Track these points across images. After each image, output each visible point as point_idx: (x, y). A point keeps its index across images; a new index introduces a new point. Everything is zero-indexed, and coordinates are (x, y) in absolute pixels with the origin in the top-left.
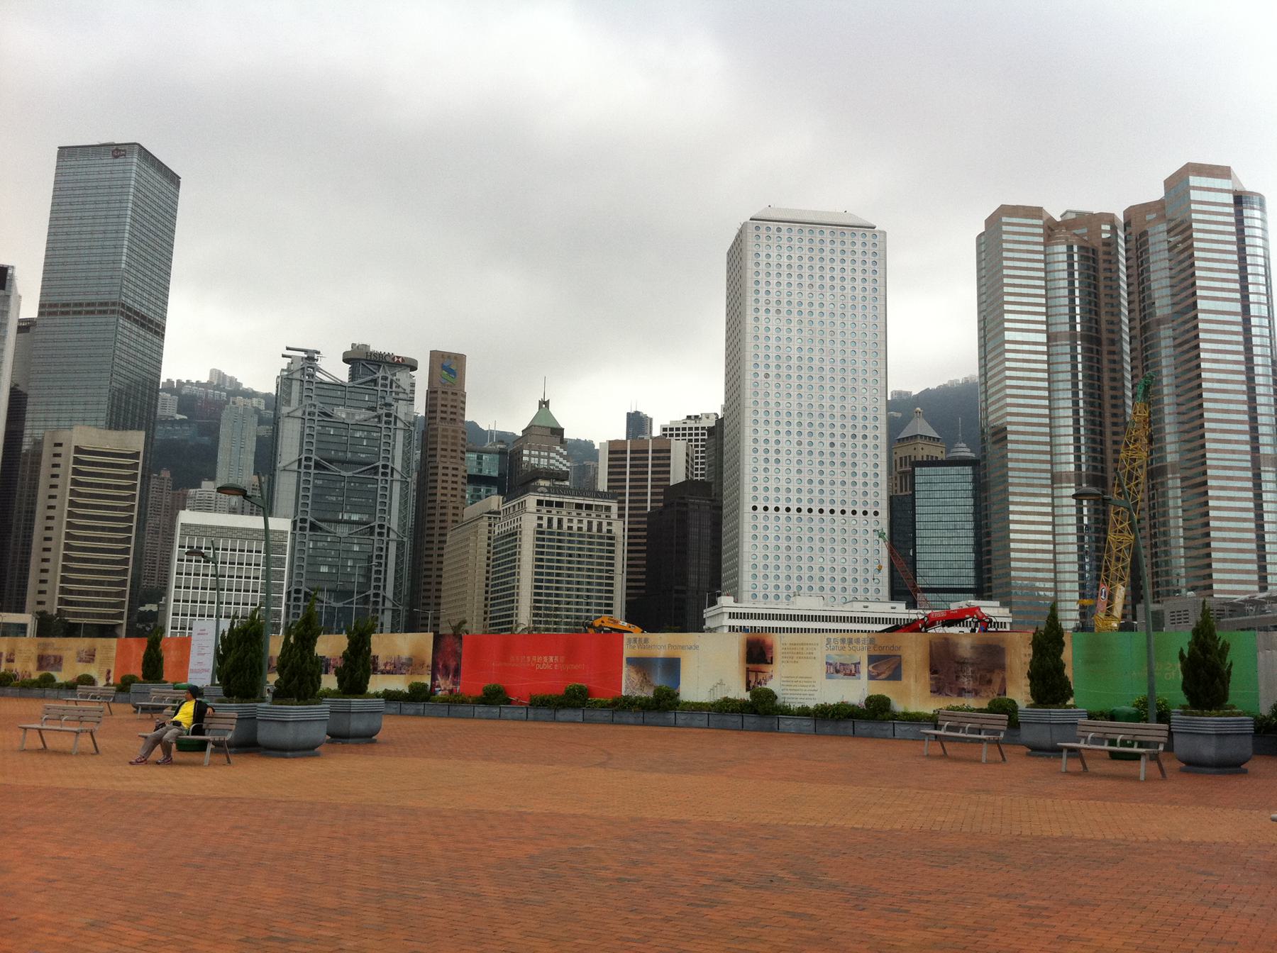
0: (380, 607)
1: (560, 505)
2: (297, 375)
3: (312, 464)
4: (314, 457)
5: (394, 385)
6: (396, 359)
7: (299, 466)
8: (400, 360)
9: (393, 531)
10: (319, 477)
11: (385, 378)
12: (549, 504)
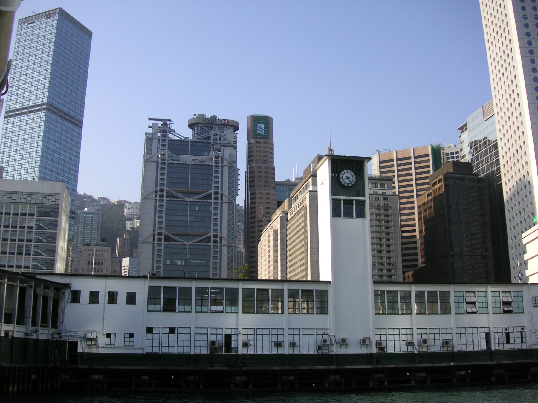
3: (165, 193)
5: (222, 139)
6: (223, 121)
8: (226, 122)
10: (170, 202)
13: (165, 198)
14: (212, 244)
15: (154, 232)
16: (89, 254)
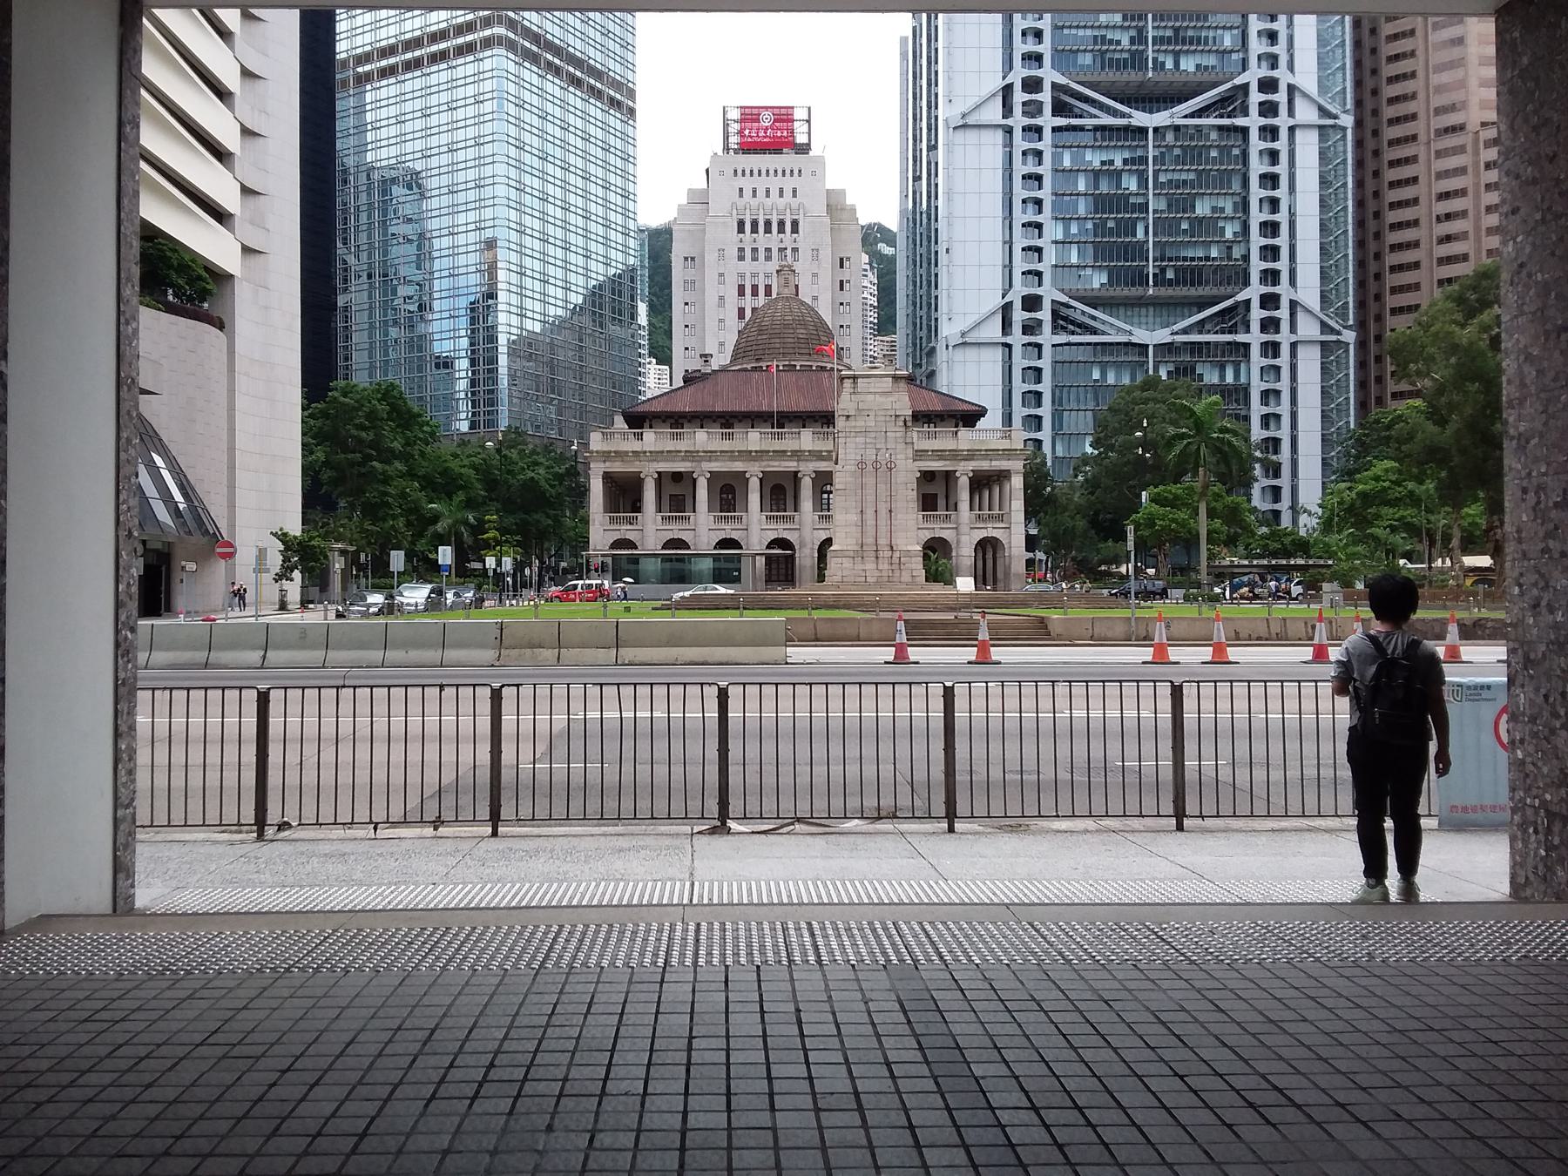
0: (1284, 337)
9: (1305, 95)
14: (1253, 121)
15: (1004, 78)
16: (741, 190)
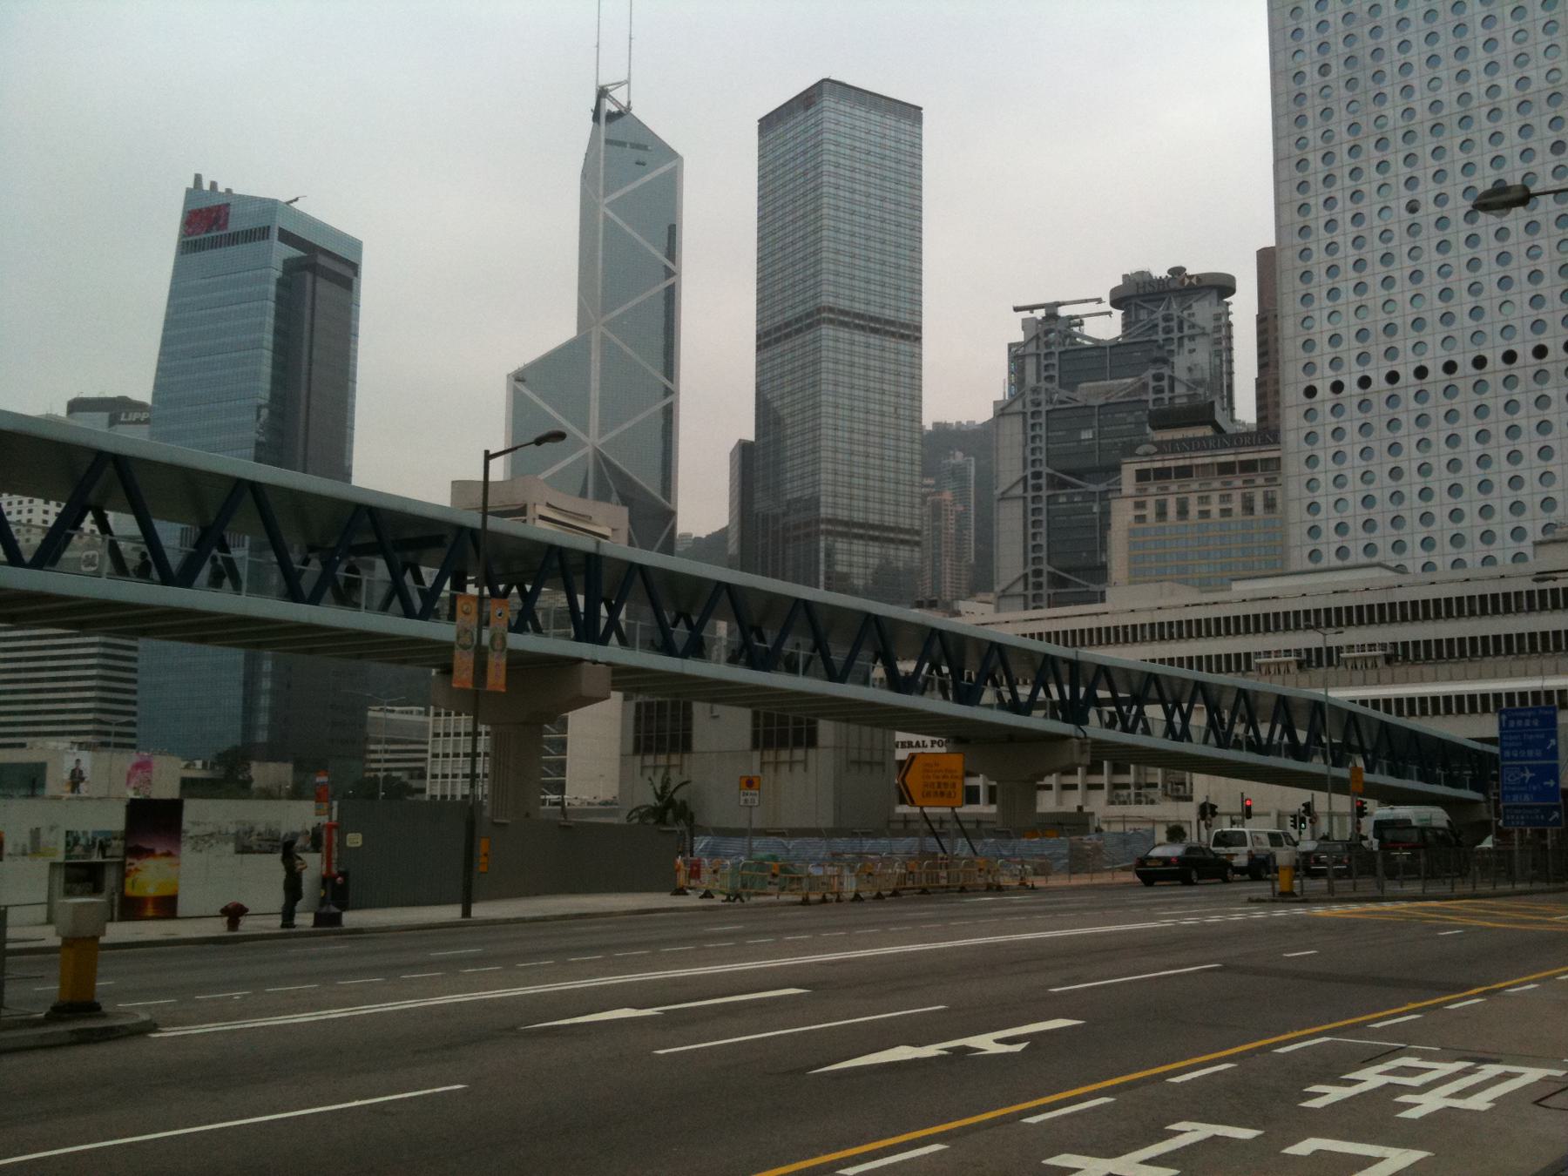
1: (1185, 472)
2: (1032, 348)
4: (1045, 470)
7: (1025, 490)
8: (1194, 281)
11: (1167, 318)
12: (1162, 474)
13: (1044, 493)
